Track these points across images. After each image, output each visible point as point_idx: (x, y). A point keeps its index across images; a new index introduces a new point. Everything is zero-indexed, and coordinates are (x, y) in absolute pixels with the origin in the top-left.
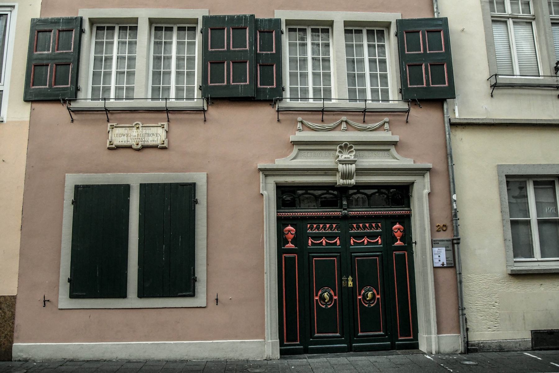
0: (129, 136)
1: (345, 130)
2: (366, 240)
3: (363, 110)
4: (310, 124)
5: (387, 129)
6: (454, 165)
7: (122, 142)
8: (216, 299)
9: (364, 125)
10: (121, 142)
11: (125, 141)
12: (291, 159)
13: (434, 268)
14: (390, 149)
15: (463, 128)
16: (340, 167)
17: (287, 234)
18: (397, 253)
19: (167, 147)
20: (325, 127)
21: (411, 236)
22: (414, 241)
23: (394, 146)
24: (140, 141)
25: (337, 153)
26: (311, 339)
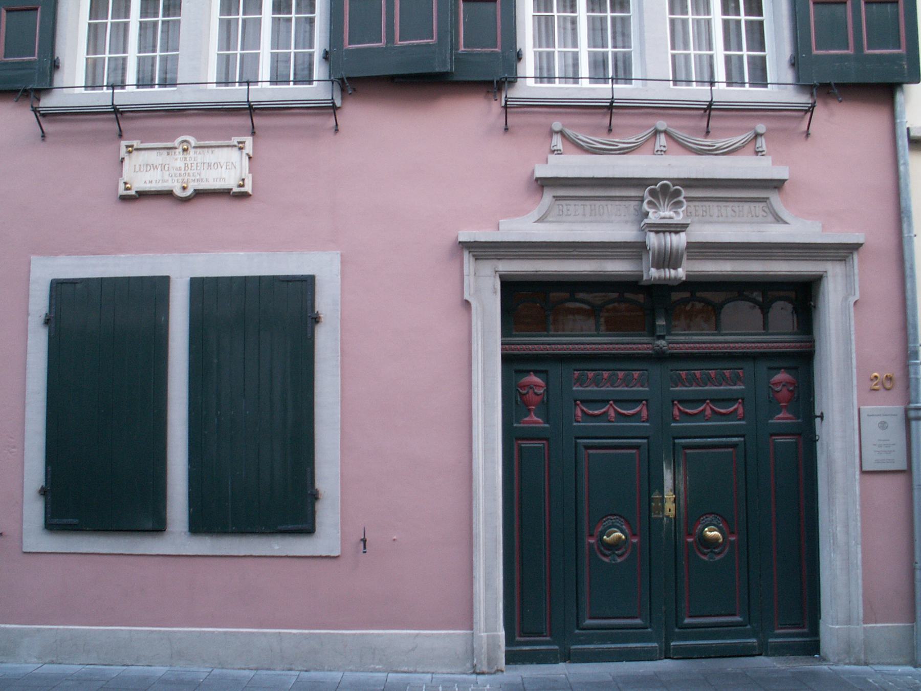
0: (166, 169)
1: (663, 153)
2: (708, 408)
3: (706, 107)
4: (580, 137)
5: (761, 152)
6: (915, 236)
7: (151, 182)
8: (362, 540)
9: (708, 141)
10: (148, 182)
11: (157, 182)
12: (535, 221)
13: (863, 472)
14: (768, 198)
16: (653, 240)
17: (524, 394)
18: (780, 440)
19: (250, 192)
20: (617, 146)
21: (812, 399)
22: (818, 413)
23: (776, 190)
24: (190, 180)
25: (645, 206)
26: (577, 631)
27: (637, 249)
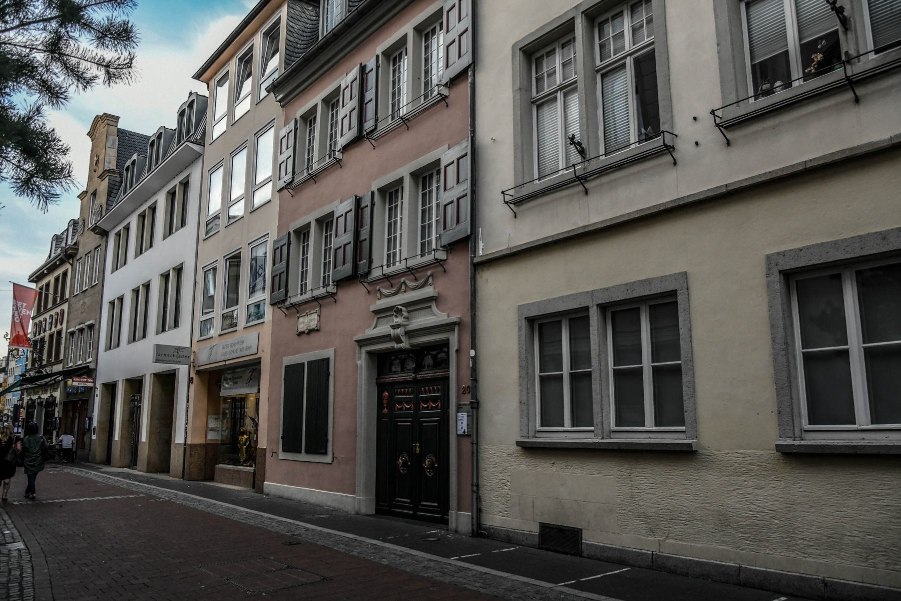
15: (490, 266)
27: (386, 338)
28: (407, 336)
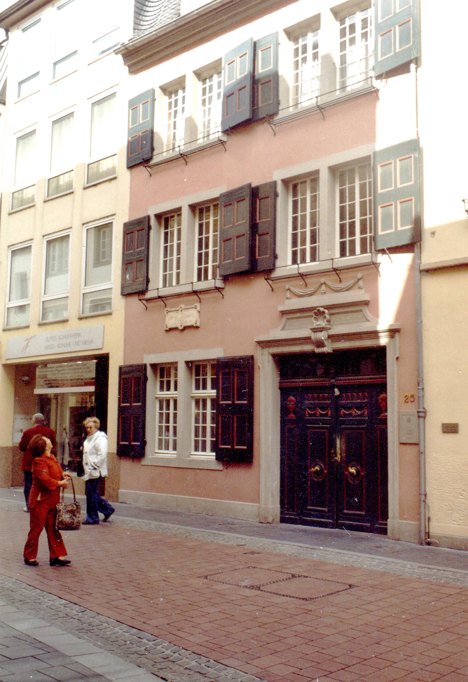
4: (296, 291)
27: (307, 340)
28: (330, 341)
